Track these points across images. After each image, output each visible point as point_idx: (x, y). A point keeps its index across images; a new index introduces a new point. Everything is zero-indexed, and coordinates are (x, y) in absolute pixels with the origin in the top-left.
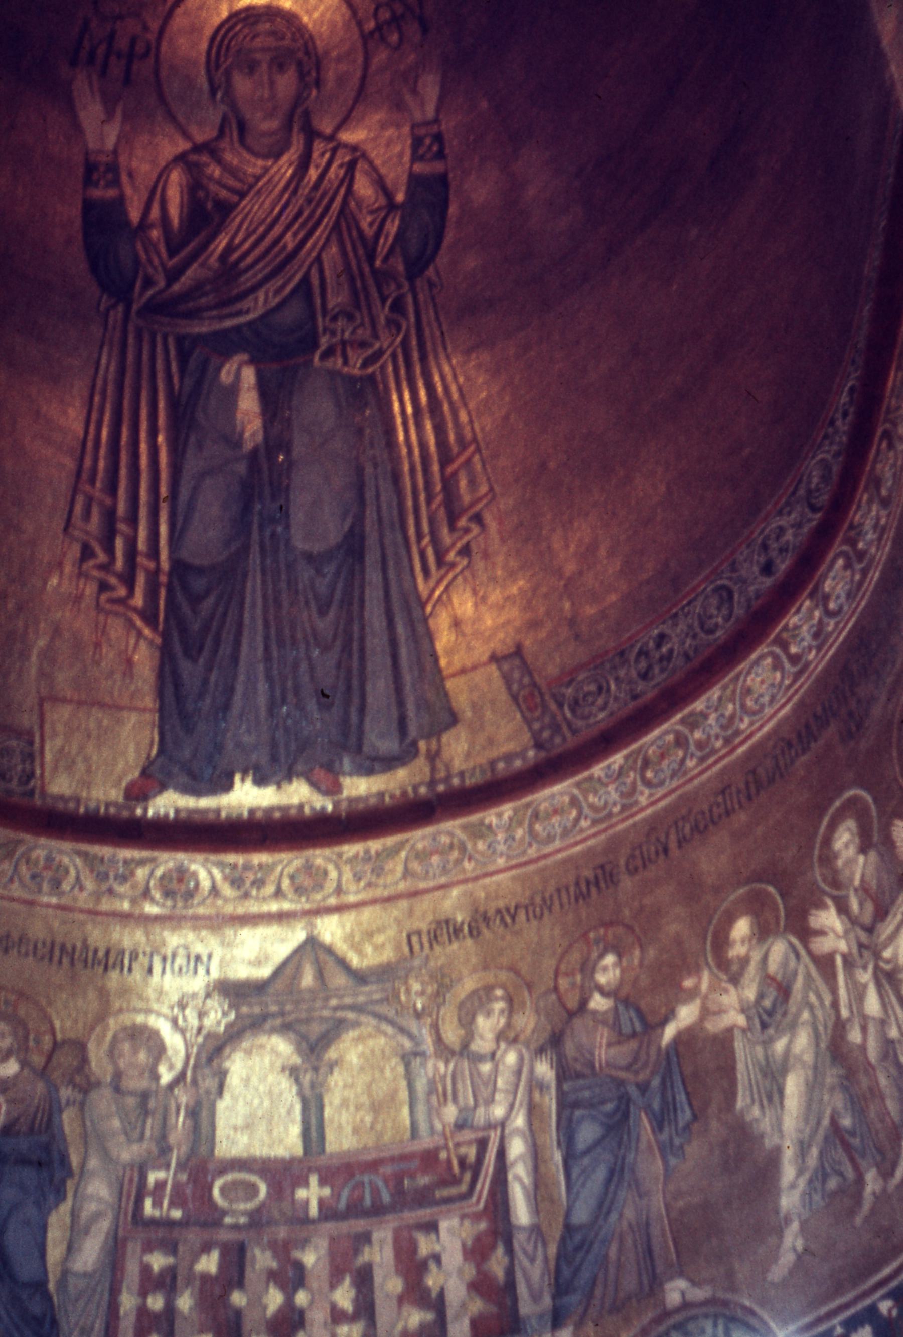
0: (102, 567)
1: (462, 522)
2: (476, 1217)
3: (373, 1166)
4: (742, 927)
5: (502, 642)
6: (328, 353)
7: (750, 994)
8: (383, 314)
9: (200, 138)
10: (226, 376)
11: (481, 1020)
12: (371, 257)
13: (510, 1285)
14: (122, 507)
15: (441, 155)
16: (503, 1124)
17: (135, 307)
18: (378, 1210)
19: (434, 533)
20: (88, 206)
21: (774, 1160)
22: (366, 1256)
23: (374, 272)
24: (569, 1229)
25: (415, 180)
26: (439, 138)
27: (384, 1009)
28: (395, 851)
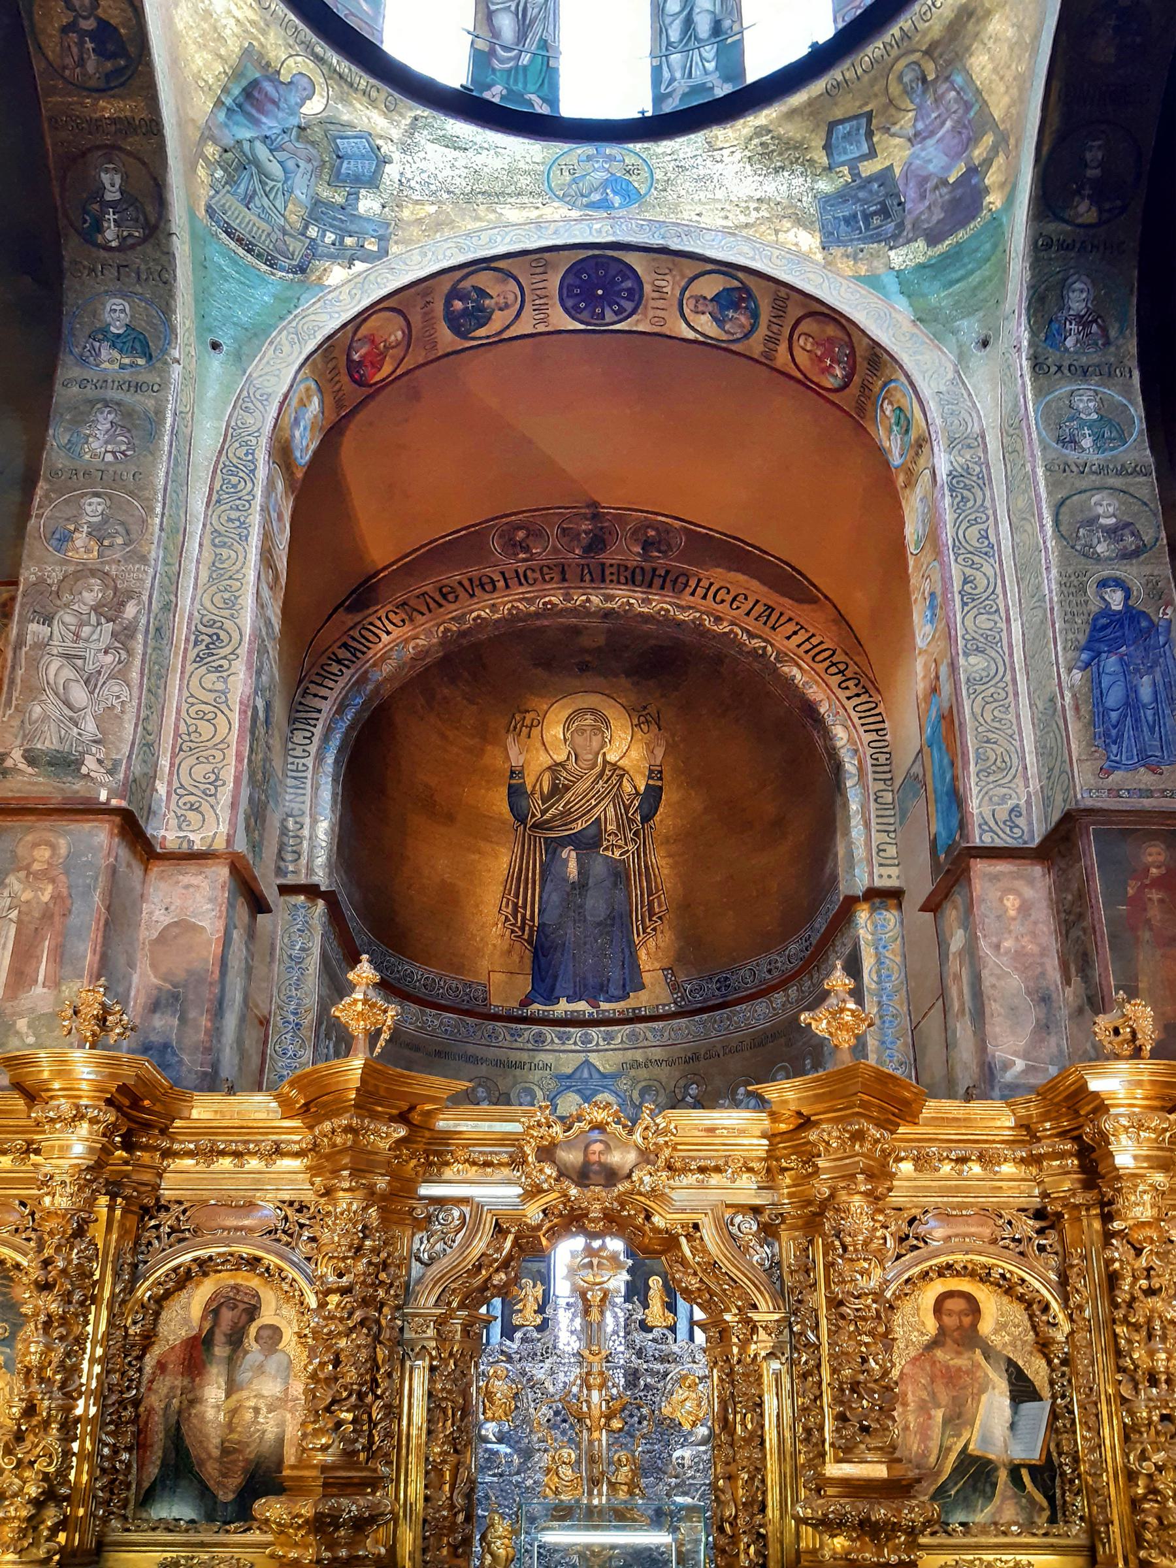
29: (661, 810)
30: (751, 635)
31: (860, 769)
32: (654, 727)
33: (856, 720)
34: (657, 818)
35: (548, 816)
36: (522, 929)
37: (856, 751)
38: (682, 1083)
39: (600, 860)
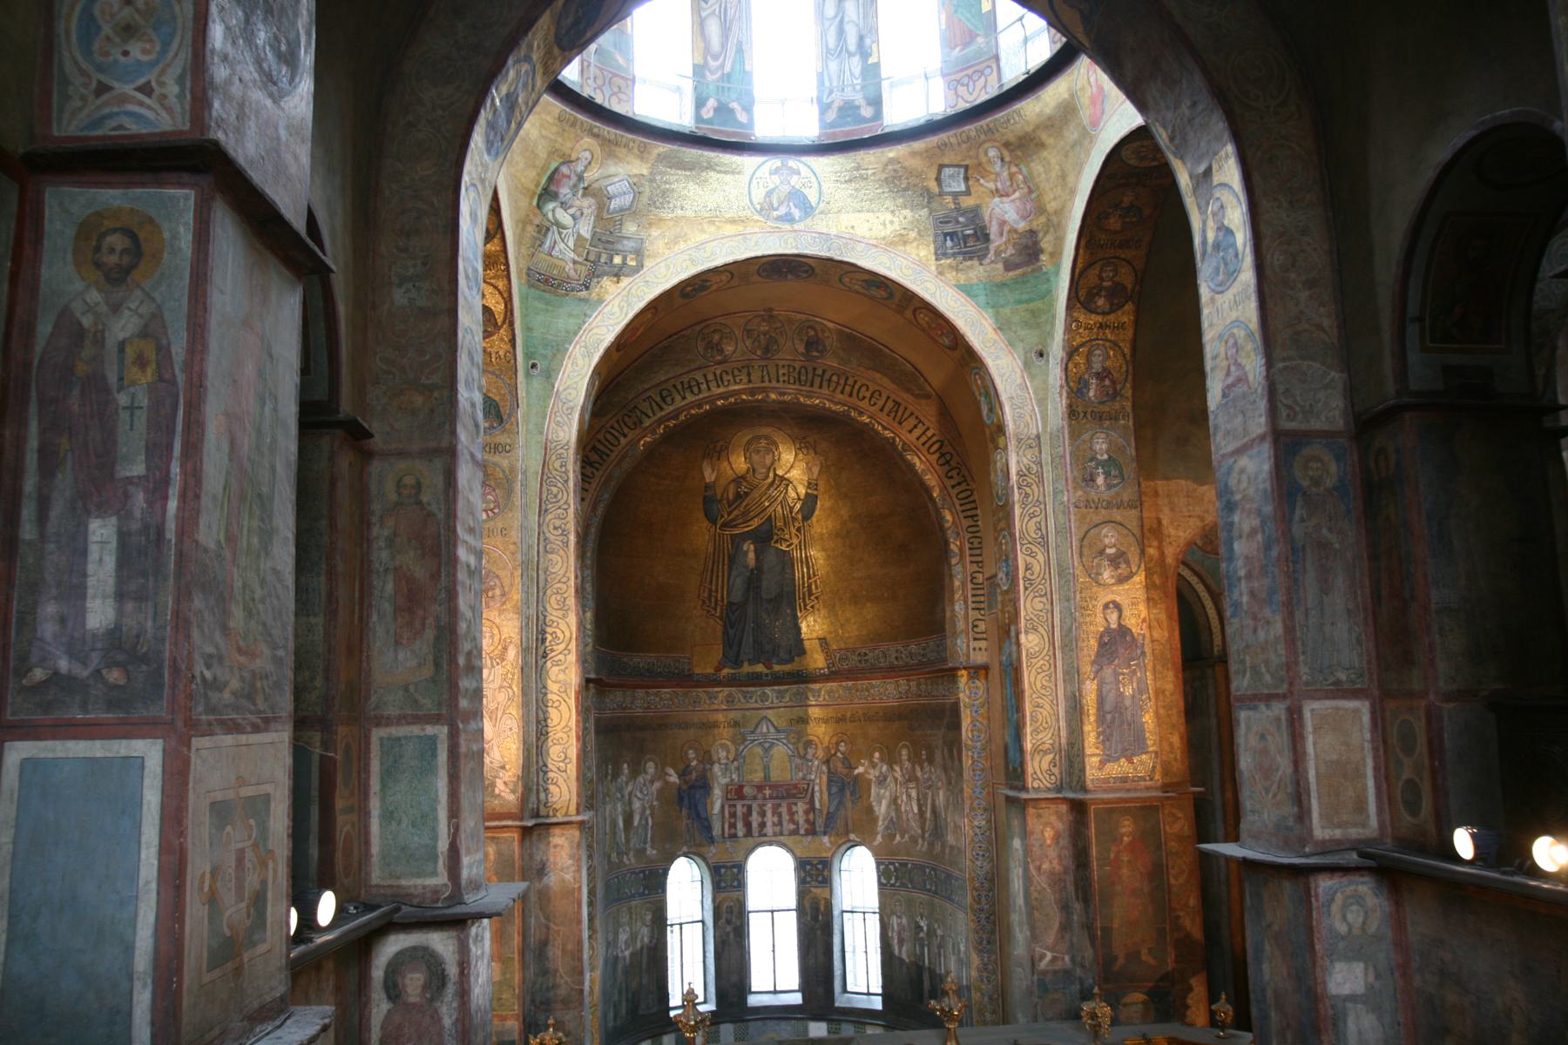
1: (812, 598)
2: (807, 803)
3: (781, 786)
4: (877, 755)
5: (821, 634)
6: (776, 542)
7: (877, 774)
8: (794, 531)
10: (745, 548)
11: (809, 750)
12: (791, 513)
13: (814, 823)
14: (714, 588)
15: (816, 489)
16: (813, 781)
18: (783, 798)
19: (804, 599)
20: (705, 497)
21: (878, 817)
22: (780, 810)
23: (793, 518)
24: (828, 813)
25: (807, 494)
26: (816, 485)
27: (785, 741)
28: (787, 691)
29: (817, 513)
30: (885, 428)
31: (961, 549)
32: (812, 451)
33: (958, 507)
34: (814, 519)
35: (733, 516)
36: (715, 609)
37: (958, 534)
38: (834, 740)
39: (772, 551)
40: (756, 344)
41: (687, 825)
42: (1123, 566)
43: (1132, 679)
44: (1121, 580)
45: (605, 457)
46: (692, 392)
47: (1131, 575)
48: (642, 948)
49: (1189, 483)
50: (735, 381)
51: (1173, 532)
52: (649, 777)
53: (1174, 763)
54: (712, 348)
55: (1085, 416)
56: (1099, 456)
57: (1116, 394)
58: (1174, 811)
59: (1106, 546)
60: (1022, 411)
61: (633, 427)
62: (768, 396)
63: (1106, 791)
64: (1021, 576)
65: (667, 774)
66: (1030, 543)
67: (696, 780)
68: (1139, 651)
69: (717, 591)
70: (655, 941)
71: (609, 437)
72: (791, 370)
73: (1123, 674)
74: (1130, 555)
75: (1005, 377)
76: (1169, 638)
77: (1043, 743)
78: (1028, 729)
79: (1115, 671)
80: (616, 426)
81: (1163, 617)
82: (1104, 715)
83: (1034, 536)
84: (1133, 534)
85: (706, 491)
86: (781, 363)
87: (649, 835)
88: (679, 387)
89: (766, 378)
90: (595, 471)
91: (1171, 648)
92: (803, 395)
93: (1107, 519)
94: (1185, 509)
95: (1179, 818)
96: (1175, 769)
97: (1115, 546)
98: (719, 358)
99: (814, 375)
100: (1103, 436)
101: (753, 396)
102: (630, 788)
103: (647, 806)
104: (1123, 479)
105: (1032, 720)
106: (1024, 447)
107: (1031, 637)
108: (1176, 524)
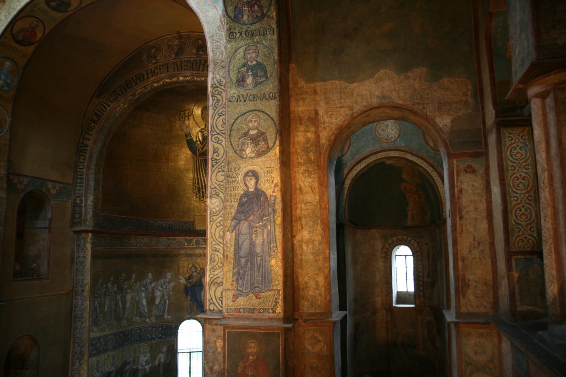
0: (199, 196)
9: (202, 128)
14: (200, 187)
17: (197, 155)
20: (187, 140)
40: (172, 52)
41: (190, 304)
42: (262, 143)
43: (263, 231)
44: (260, 154)
45: (100, 118)
46: (140, 80)
47: (268, 149)
48: (159, 365)
49: (342, 82)
50: (160, 72)
51: (327, 119)
52: (168, 280)
53: (319, 298)
54: (151, 57)
55: (241, 35)
56: (249, 63)
57: (263, 16)
58: (316, 335)
59: (250, 129)
60: (218, 44)
61: (113, 101)
62: (178, 78)
63: (237, 318)
64: (210, 157)
65: (179, 279)
66: (218, 134)
67: (196, 282)
68: (270, 209)
69: (202, 188)
70: (168, 361)
71: (102, 107)
72: (189, 62)
73: (256, 227)
74: (268, 135)
75: (211, 23)
76: (320, 200)
77: (218, 277)
78: (208, 267)
79: (250, 224)
80: (106, 102)
81: (316, 184)
82: (239, 260)
83: (221, 128)
84: (272, 119)
85: (186, 137)
86: (184, 60)
87: (167, 308)
88: (134, 78)
89: (176, 69)
90: (95, 125)
91: (321, 208)
92: (195, 76)
93: (253, 108)
94: (337, 102)
95: (320, 341)
96: (319, 303)
97: (256, 128)
98: (154, 61)
99: (200, 64)
100: (254, 48)
101: (171, 80)
102: (153, 285)
103: (165, 294)
104: (267, 78)
105: (211, 260)
106: (218, 68)
107: (214, 200)
108: (329, 113)
